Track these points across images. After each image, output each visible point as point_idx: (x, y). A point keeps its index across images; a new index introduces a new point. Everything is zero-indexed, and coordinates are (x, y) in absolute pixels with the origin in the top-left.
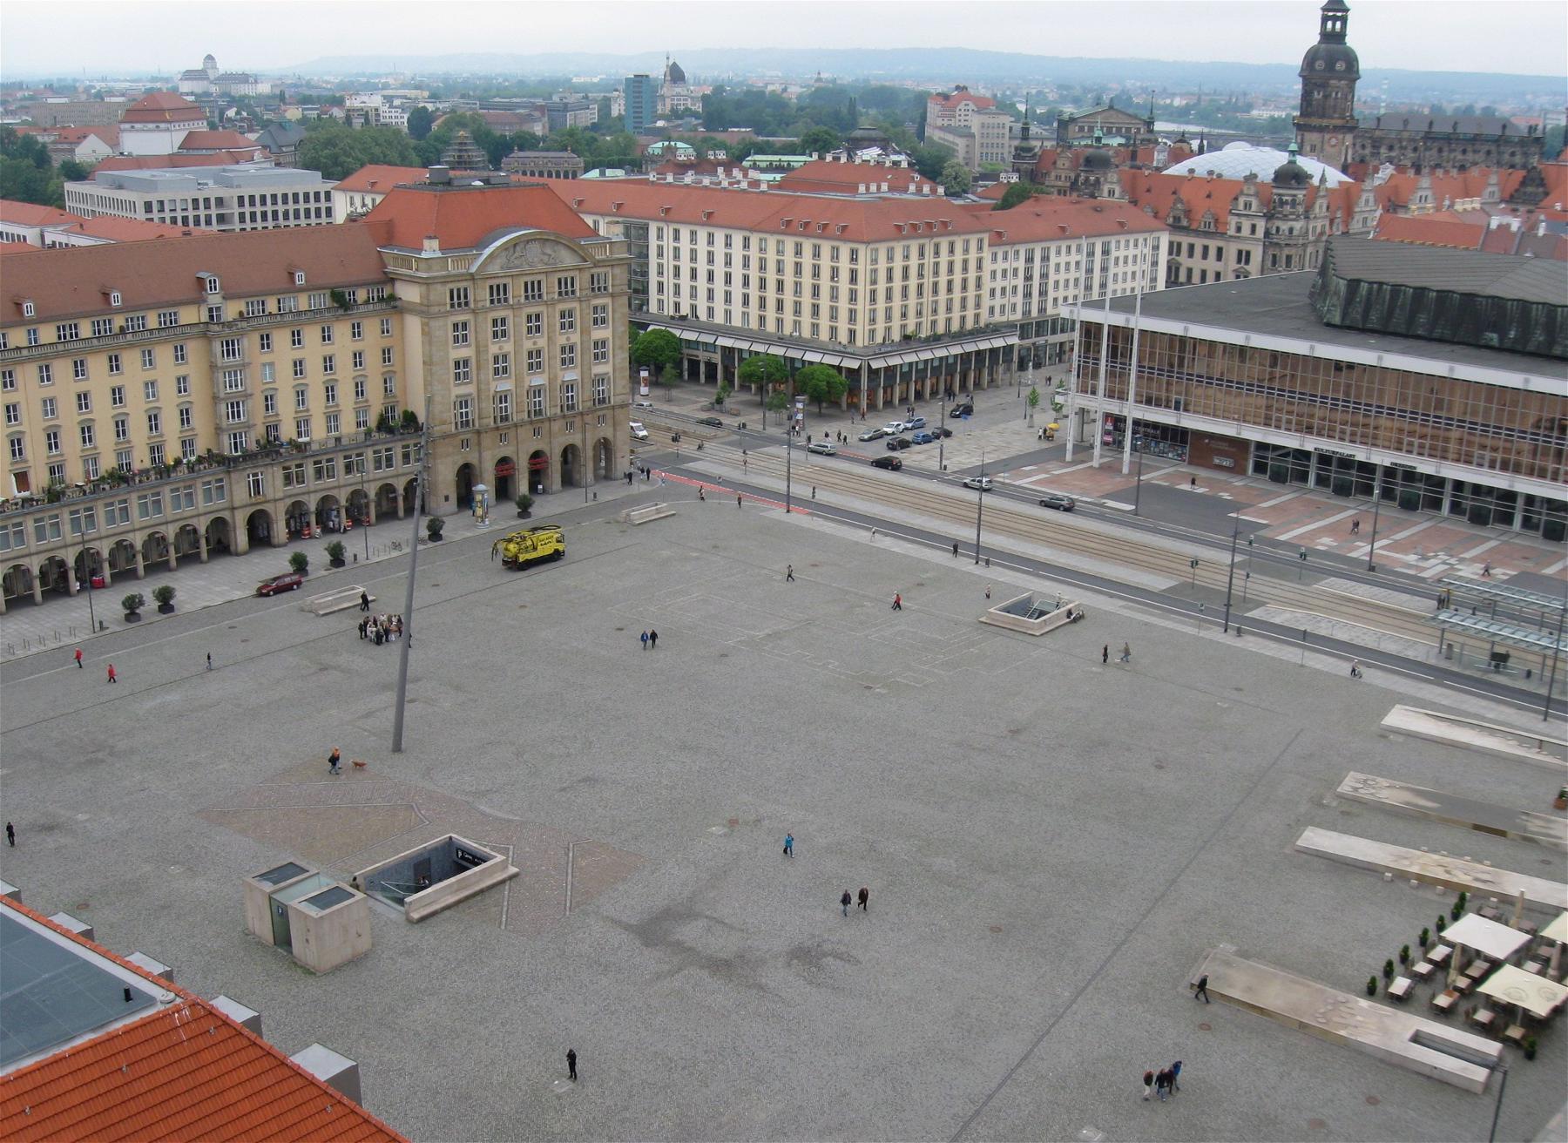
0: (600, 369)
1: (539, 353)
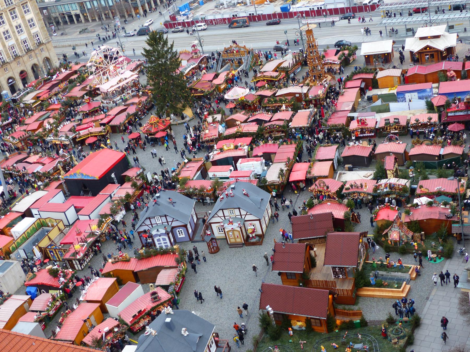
0: (34, 30)
1: (7, 31)
